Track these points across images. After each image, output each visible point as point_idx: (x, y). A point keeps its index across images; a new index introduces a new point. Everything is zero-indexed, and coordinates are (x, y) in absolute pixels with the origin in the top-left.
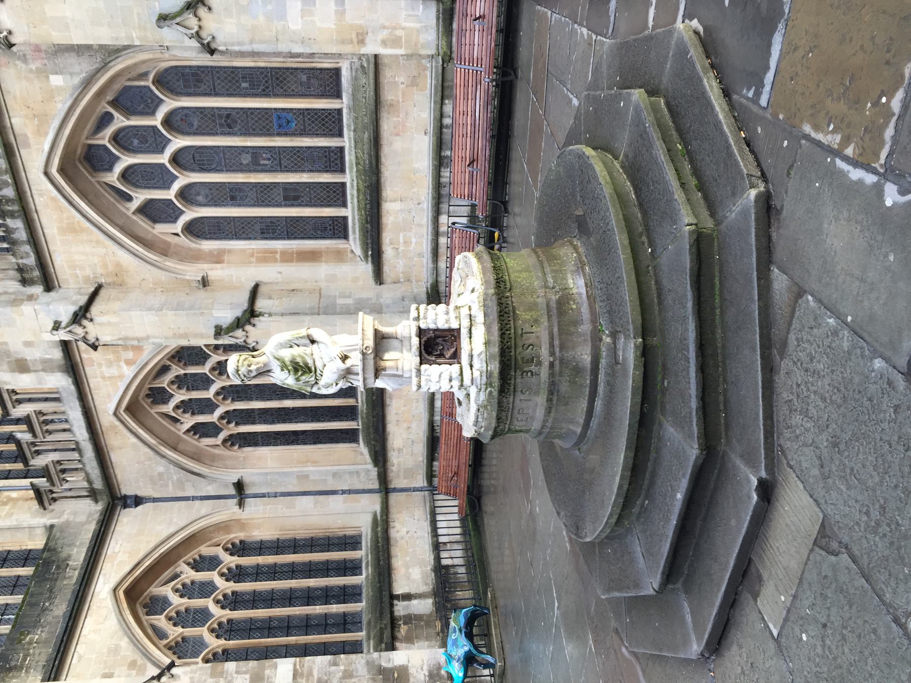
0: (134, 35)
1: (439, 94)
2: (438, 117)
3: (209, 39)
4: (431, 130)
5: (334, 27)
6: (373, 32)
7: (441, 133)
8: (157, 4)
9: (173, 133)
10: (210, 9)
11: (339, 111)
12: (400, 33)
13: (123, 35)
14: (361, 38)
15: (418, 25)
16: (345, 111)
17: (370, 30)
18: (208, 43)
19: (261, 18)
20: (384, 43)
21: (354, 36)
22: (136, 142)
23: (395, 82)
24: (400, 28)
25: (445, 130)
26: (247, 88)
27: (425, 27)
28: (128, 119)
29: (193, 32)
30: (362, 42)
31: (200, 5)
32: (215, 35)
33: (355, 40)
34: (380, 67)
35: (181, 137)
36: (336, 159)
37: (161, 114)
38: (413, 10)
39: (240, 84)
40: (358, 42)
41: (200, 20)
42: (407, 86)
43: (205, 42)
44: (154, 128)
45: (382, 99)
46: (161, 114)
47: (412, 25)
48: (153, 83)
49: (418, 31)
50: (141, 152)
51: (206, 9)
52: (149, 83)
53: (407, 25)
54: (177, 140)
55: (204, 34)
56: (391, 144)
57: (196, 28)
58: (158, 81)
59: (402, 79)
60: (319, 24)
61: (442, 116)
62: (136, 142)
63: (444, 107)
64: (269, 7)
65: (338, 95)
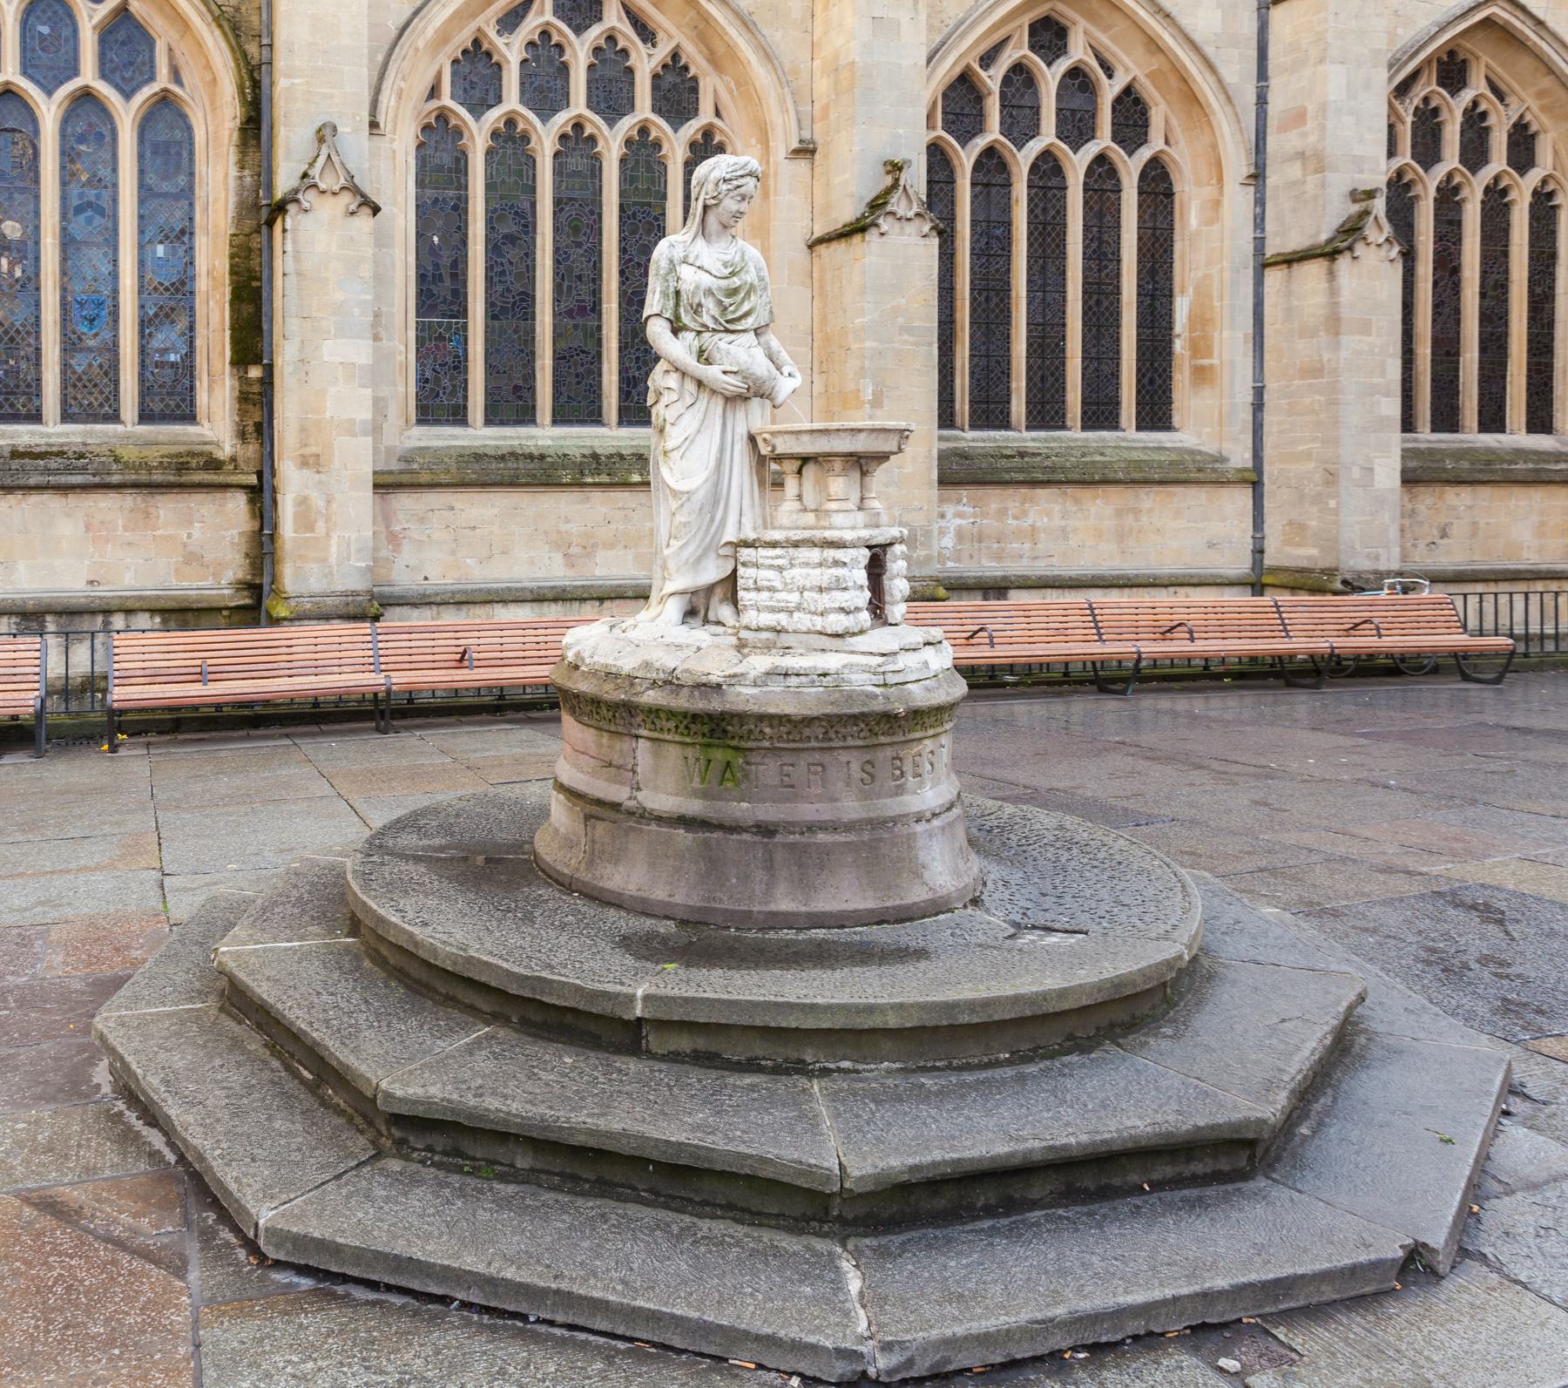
0: (297, 81)
1: (173, 605)
2: (130, 604)
3: (306, 205)
4: (103, 592)
5: (328, 415)
6: (320, 482)
7: (93, 613)
8: (348, 130)
9: (66, 104)
10: (352, 213)
11: (115, 417)
12: (321, 527)
13: (298, 63)
14: (311, 460)
15: (333, 560)
16: (119, 428)
17: (323, 477)
18: (297, 201)
19: (339, 296)
20: (303, 502)
21: (313, 450)
22: (45, 30)
23: (191, 523)
24: (328, 529)
25: (100, 619)
26: (155, 252)
27: (331, 573)
28: (94, 28)
29: (317, 179)
30: (305, 462)
31: (359, 199)
32: (310, 215)
33: (307, 451)
34: (219, 495)
35: (59, 117)
36: (12, 406)
37: (104, 89)
38: (359, 551)
39: (161, 242)
40: (303, 456)
41: (334, 194)
42: (185, 545)
43: (300, 196)
44: (75, 72)
45: (159, 497)
46: (104, 89)
47: (334, 549)
48: (165, 90)
49: (324, 560)
50: (23, 36)
51: (353, 207)
52: (163, 80)
53: (334, 541)
54: (54, 108)
55: (309, 198)
56: (68, 515)
57: (323, 186)
58: (165, 100)
59: (196, 534)
60: (332, 390)
61: (129, 612)
62: (45, 30)
63: (147, 615)
64: (357, 311)
65: (145, 417)
